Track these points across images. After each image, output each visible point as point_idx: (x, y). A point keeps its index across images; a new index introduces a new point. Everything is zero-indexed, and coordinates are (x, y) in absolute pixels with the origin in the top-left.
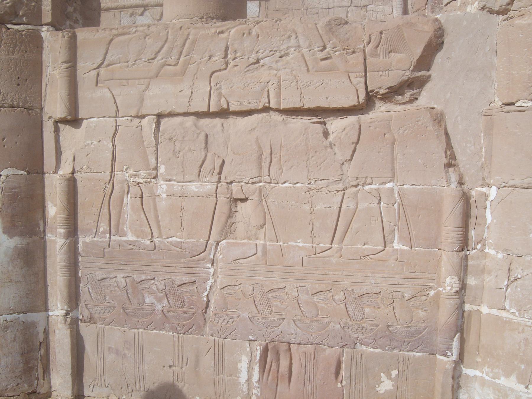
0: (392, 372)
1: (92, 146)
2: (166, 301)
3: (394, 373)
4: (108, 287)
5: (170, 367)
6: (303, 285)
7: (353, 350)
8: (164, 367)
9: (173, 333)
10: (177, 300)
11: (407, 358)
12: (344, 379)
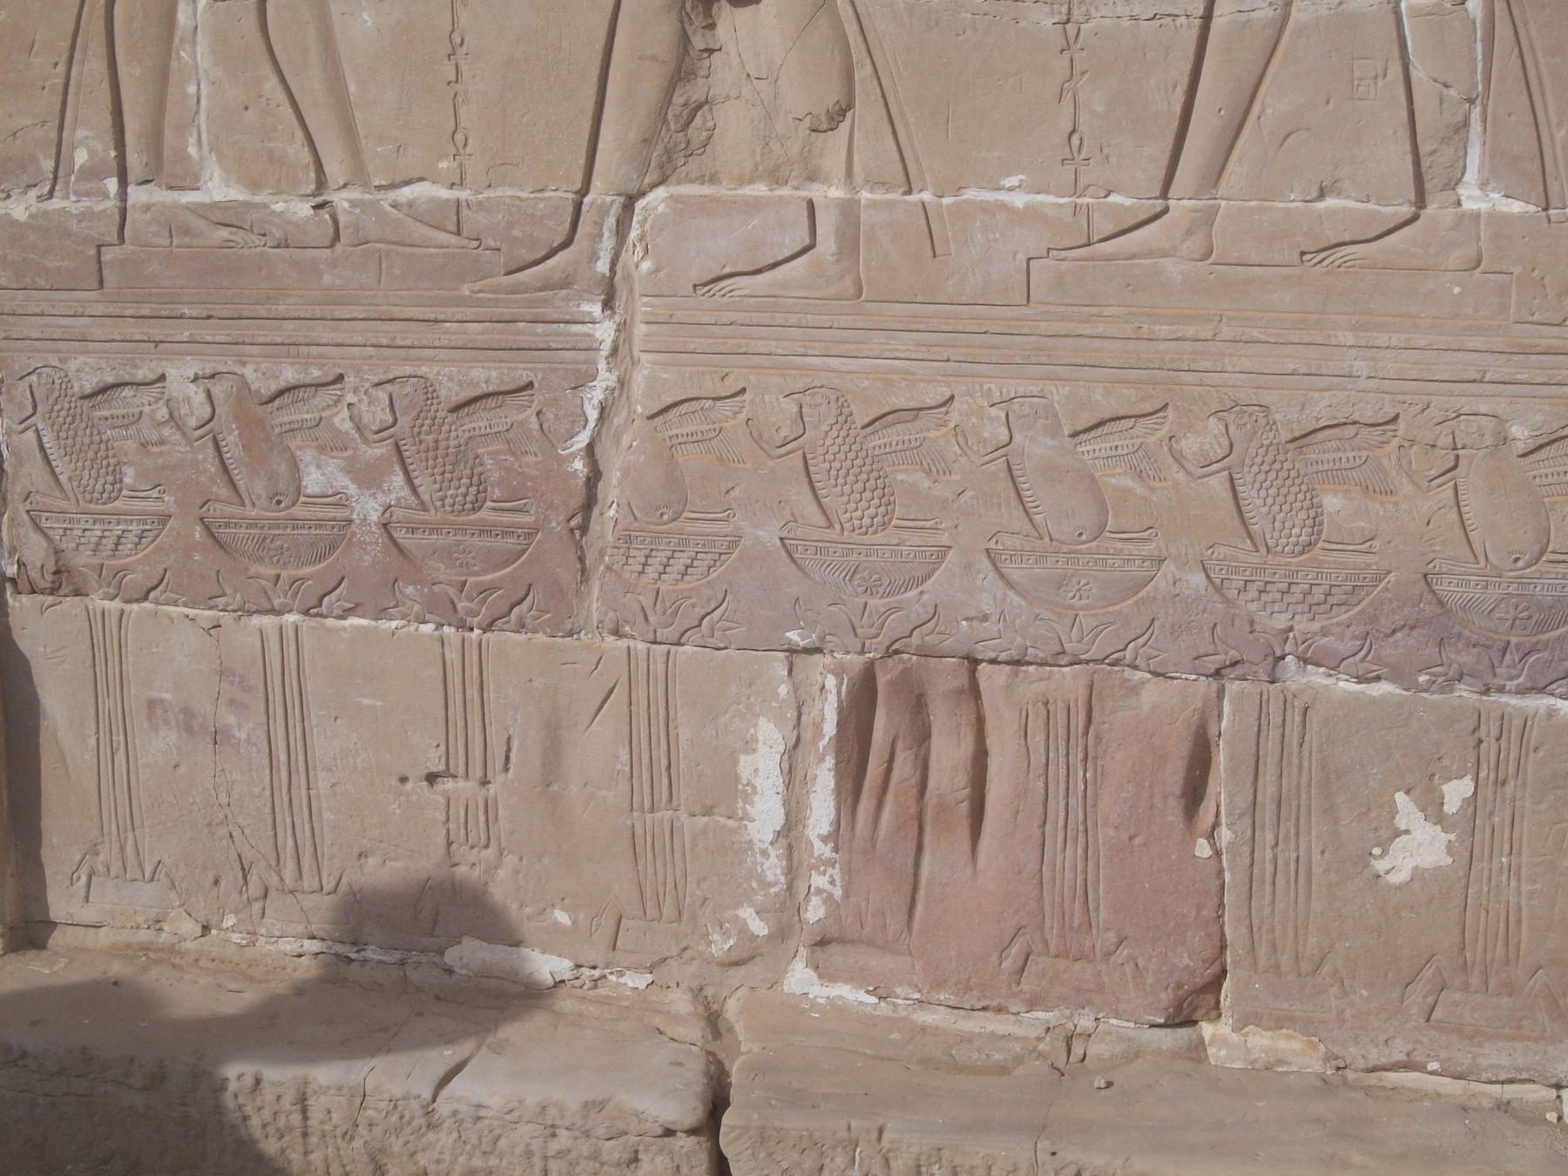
0: (1446, 788)
2: (398, 479)
3: (1456, 792)
4: (126, 427)
5: (432, 778)
6: (1034, 389)
7: (1265, 686)
8: (404, 780)
9: (440, 626)
10: (448, 476)
11: (1517, 723)
12: (1223, 820)
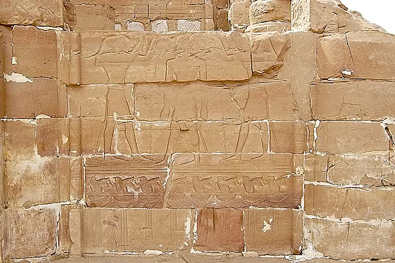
1: (93, 101)
3: (271, 220)
